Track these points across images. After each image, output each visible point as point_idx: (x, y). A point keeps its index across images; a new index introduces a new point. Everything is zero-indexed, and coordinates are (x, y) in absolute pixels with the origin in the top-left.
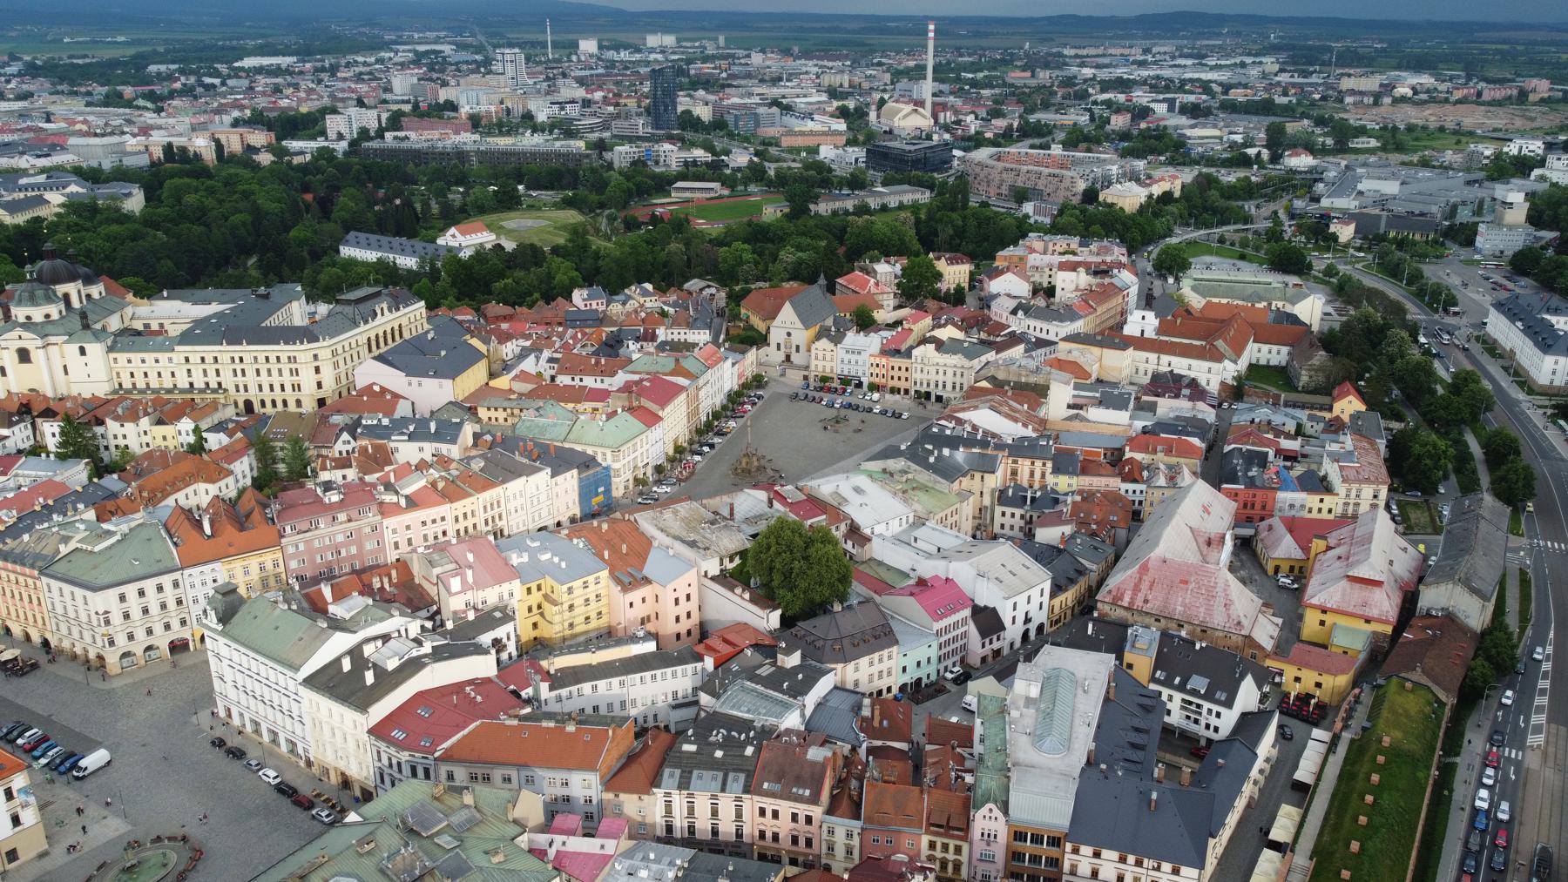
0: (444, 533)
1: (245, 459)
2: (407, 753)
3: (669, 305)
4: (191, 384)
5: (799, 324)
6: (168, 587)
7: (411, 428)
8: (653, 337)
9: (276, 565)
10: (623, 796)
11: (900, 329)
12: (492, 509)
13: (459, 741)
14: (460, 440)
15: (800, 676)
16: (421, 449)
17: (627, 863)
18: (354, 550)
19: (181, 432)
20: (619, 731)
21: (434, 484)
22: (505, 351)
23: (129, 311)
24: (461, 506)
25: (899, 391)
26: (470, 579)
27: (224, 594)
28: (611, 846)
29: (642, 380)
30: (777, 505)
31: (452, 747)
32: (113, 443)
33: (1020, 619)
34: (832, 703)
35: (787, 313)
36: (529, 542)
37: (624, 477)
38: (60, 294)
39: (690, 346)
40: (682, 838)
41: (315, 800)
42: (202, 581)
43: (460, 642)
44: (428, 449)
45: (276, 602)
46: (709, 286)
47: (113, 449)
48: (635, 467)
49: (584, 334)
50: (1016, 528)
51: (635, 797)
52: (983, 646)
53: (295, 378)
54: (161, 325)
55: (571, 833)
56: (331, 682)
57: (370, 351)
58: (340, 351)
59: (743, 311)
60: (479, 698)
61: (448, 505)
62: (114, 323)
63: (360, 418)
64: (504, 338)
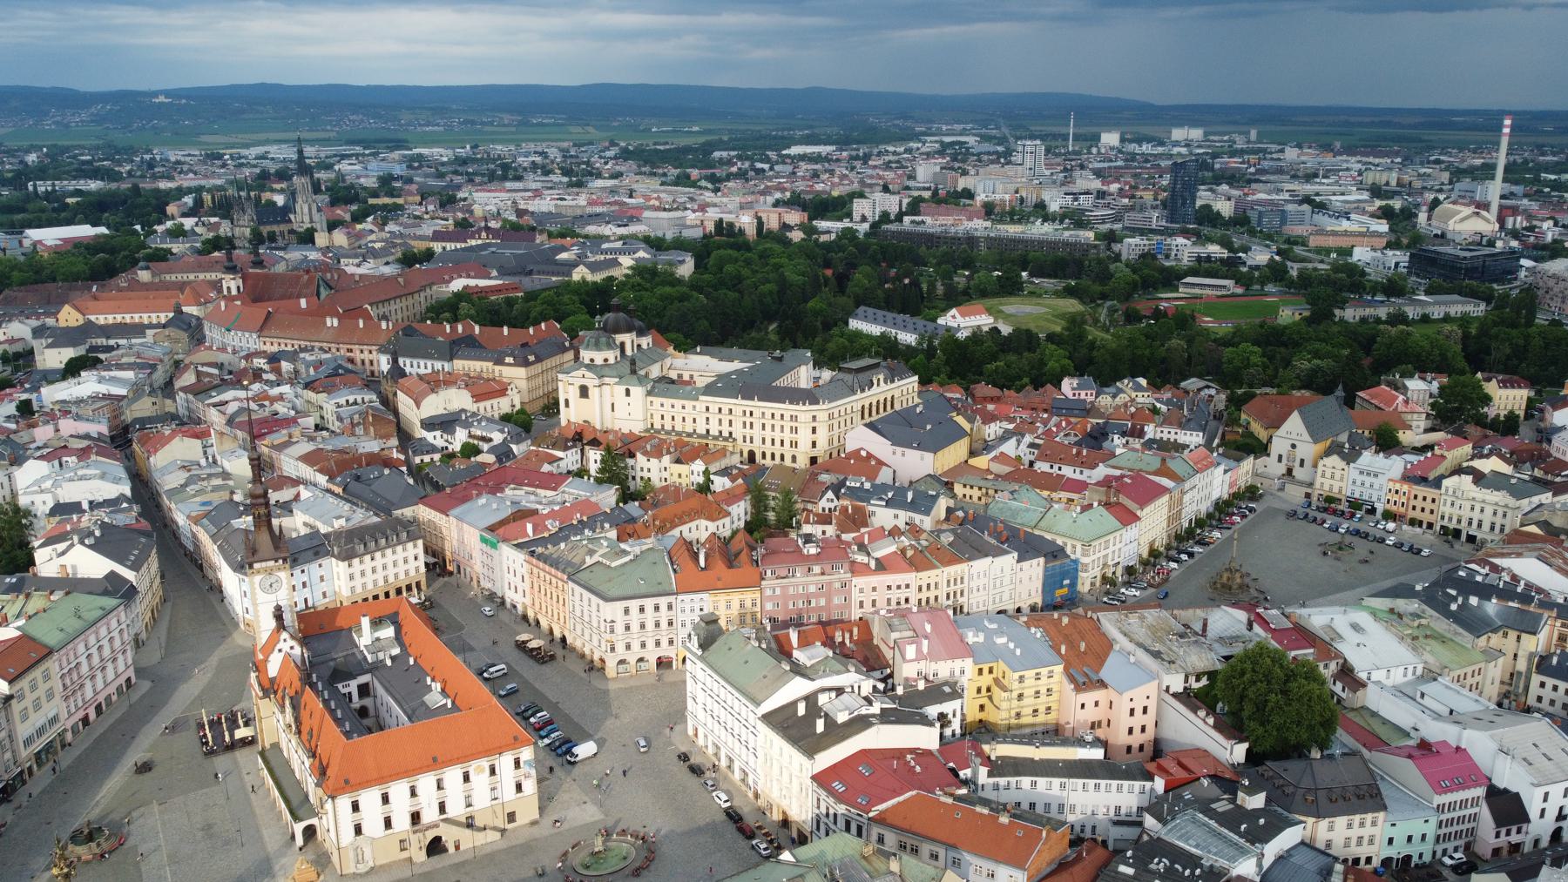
0: (907, 600)
1: (742, 504)
2: (843, 807)
3: (1162, 402)
4: (708, 431)
5: (1306, 436)
6: (663, 607)
8: (1141, 434)
9: (754, 605)
11: (1429, 454)
12: (955, 584)
13: (894, 807)
14: (933, 513)
15: (1262, 821)
16: (896, 516)
18: (823, 602)
20: (1053, 834)
21: (903, 551)
22: (988, 431)
23: (668, 361)
24: (926, 577)
25: (1420, 524)
27: (707, 623)
29: (1122, 476)
30: (1257, 628)
32: (639, 474)
33: (1552, 814)
34: (1297, 859)
35: (1294, 423)
36: (986, 623)
37: (1091, 574)
38: (618, 343)
39: (1180, 447)
41: (757, 832)
42: (691, 607)
43: (907, 709)
44: (904, 516)
46: (1208, 387)
47: (638, 479)
48: (1105, 565)
49: (1069, 423)
50: (1558, 705)
52: (1498, 835)
53: (794, 435)
54: (691, 377)
56: (789, 724)
57: (863, 418)
58: (836, 415)
59: (1243, 416)
60: (918, 769)
61: (914, 574)
62: (655, 371)
63: (846, 479)
64: (989, 418)
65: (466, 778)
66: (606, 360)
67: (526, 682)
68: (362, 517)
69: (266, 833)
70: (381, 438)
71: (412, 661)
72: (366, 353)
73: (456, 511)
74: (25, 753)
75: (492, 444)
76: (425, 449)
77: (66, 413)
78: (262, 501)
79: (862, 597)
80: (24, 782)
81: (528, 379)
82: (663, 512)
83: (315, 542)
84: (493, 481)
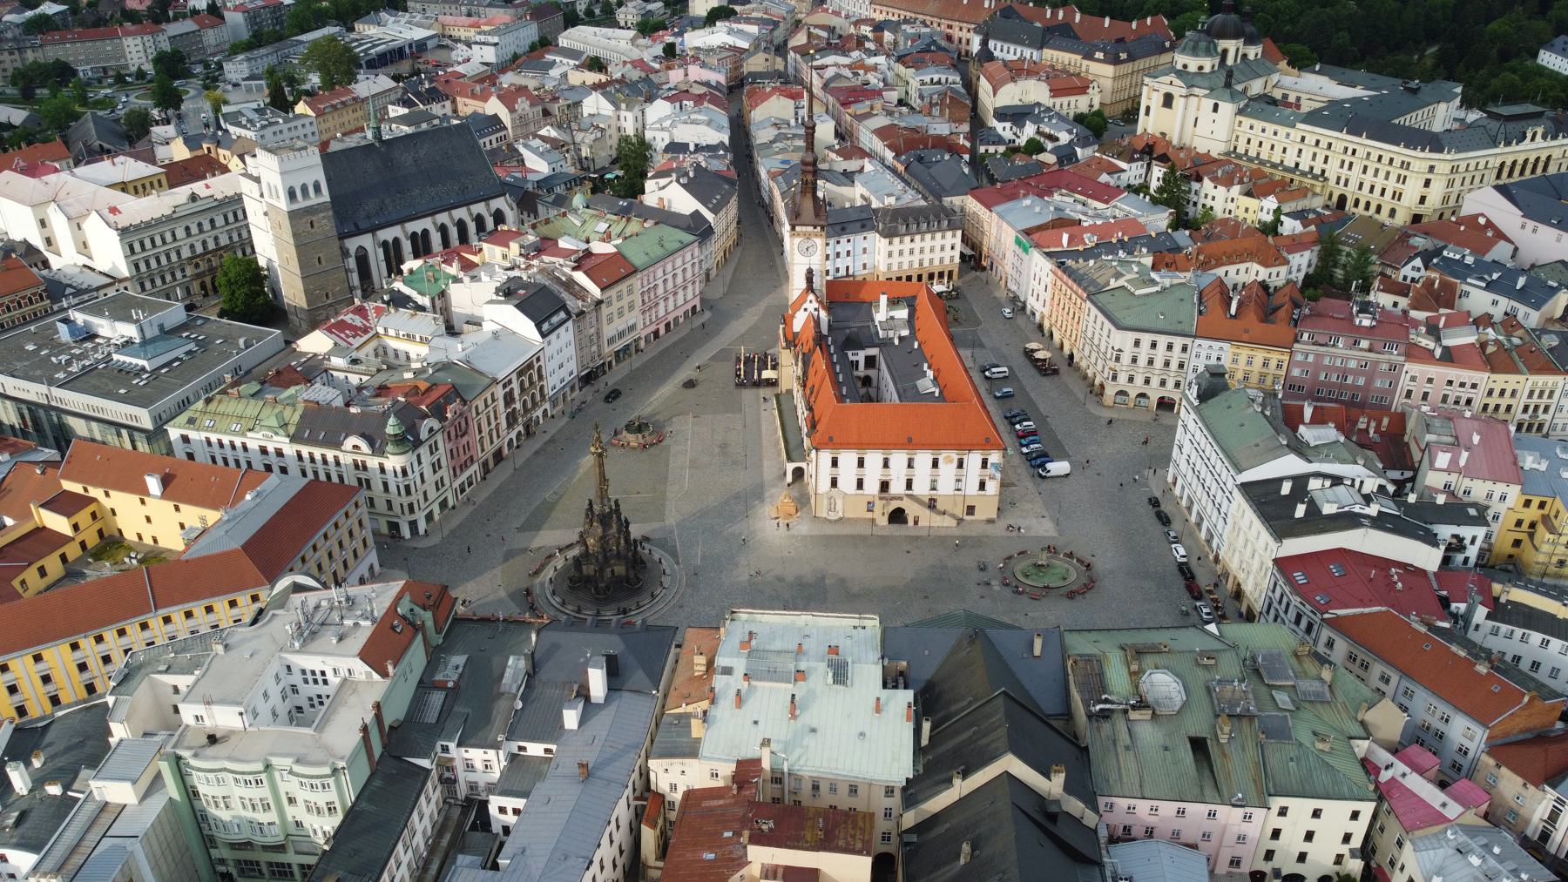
0: (1469, 402)
1: (1307, 254)
2: (1299, 599)
6: (1177, 348)
7: (1495, 276)
9: (1279, 366)
10: (1504, 770)
12: (1541, 395)
13: (1354, 616)
14: (1545, 308)
16: (1495, 303)
17: (1463, 838)
18: (1361, 381)
19: (1262, 209)
20: (1538, 703)
21: (1483, 345)
23: (1275, 78)
24: (1501, 380)
26: (1462, 462)
27: (1212, 375)
28: (1453, 810)
31: (1346, 617)
32: (1202, 201)
36: (1558, 451)
38: (1219, 49)
40: (1555, 857)
41: (1206, 595)
42: (1206, 353)
44: (1505, 304)
45: (1253, 400)
47: (1200, 206)
51: (1520, 781)
53: (1399, 185)
54: (1298, 99)
55: (1421, 771)
56: (1265, 498)
57: (1498, 176)
60: (1400, 585)
61: (1488, 374)
62: (1256, 87)
63: (1444, 247)
65: (935, 464)
66: (1201, 68)
67: (1022, 388)
68: (912, 199)
69: (766, 464)
70: (954, 122)
71: (916, 345)
72: (965, 30)
73: (998, 208)
74: (607, 349)
75: (1057, 144)
76: (992, 139)
77: (695, 59)
78: (810, 168)
79: (1412, 386)
80: (605, 373)
81: (1114, 78)
82: (1213, 247)
83: (864, 216)
84: (1042, 183)
